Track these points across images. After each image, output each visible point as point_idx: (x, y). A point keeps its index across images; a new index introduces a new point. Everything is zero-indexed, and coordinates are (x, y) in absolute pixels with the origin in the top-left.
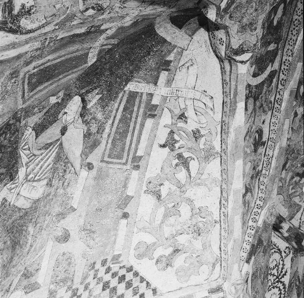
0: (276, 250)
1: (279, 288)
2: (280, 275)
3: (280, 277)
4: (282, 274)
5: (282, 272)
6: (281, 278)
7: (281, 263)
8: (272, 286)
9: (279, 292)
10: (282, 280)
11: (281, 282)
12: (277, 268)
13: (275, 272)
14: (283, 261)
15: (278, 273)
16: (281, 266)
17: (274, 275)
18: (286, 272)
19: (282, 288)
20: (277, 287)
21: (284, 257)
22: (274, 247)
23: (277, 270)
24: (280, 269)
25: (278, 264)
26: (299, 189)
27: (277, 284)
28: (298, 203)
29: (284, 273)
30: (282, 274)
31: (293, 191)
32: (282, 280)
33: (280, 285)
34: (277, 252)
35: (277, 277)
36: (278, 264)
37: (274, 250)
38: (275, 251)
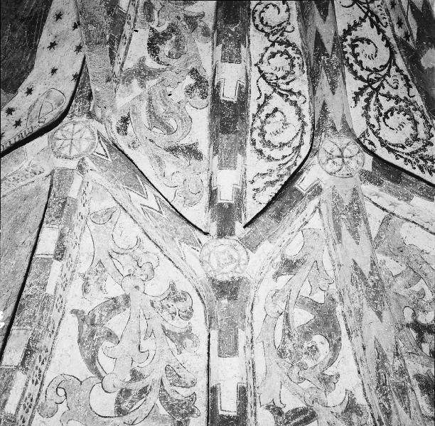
0: (400, 149)
1: (362, 69)
2: (371, 95)
3: (369, 90)
4: (365, 96)
5: (367, 100)
6: (366, 87)
7: (373, 121)
8: (383, 73)
9: (359, 59)
10: (361, 84)
11: (361, 78)
12: (383, 112)
13: (387, 105)
14: (368, 123)
15: (377, 100)
16: (373, 113)
17: (388, 96)
18: (356, 100)
19: (356, 67)
20: (368, 69)
21: (370, 131)
22: (409, 157)
23: (381, 106)
24: (372, 107)
25: (381, 118)
26: (402, 293)
27: (372, 77)
28: (388, 258)
29: (362, 99)
30: (365, 96)
31: (416, 288)
32: (361, 84)
33: (365, 74)
34: (393, 145)
35: (377, 90)
36: (381, 118)
37: (405, 151)
38: (403, 147)
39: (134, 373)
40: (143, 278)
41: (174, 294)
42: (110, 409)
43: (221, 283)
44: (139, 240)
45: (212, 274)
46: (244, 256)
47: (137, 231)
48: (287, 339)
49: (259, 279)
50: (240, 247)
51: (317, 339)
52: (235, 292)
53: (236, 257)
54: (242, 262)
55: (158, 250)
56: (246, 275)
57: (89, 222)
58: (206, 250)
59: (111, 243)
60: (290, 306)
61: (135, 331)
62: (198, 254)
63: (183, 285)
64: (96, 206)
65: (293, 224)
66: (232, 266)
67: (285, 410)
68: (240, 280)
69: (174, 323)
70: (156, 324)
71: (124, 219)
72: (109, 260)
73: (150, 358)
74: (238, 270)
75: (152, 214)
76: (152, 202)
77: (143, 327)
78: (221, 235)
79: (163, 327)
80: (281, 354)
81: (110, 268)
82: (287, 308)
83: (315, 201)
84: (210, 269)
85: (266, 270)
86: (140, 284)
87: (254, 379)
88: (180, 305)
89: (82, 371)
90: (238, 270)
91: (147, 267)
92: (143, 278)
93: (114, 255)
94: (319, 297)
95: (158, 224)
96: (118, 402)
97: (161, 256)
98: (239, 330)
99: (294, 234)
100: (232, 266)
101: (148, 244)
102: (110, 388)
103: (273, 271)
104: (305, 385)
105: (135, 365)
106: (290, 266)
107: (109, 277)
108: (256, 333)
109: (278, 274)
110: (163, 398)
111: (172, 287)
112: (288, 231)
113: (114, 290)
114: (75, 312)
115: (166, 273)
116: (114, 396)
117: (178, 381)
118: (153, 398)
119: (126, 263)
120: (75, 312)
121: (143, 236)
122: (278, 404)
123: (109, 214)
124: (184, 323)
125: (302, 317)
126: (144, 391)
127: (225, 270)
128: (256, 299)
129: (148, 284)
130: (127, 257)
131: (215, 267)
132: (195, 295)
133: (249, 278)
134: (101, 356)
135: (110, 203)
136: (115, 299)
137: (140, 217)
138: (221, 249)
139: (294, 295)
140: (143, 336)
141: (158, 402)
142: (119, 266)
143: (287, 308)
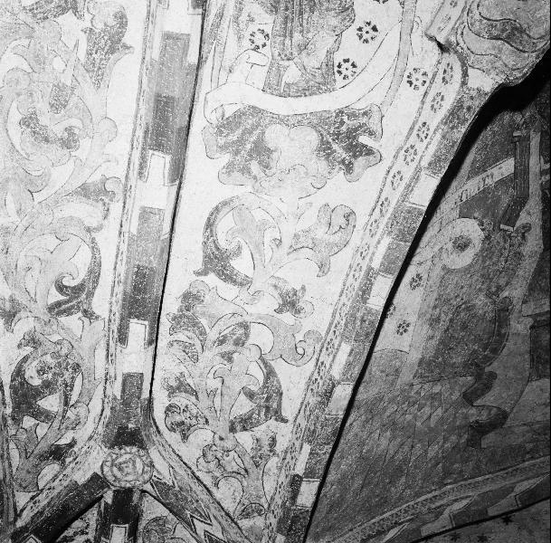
39: (230, 360)
40: (214, 448)
41: (184, 430)
42: (254, 329)
43: (134, 444)
44: (216, 485)
45: (142, 453)
46: (106, 469)
47: (218, 494)
48: (69, 381)
49: (92, 442)
50: (111, 479)
51: (36, 382)
52: (119, 435)
53: (115, 469)
54: (108, 464)
55: (198, 474)
56: (106, 450)
57: (266, 506)
58: (147, 477)
59: (245, 484)
60: (61, 414)
61: (226, 398)
62: (155, 473)
63: (173, 438)
64: (259, 522)
65: (48, 500)
66: (120, 460)
67: (80, 314)
68: (112, 447)
69: (185, 402)
70: (204, 402)
71: (229, 505)
72: (248, 467)
73: (213, 371)
74: (114, 456)
75: (201, 516)
76: (200, 527)
77: (217, 399)
78: (129, 491)
79: (197, 398)
80: (77, 367)
81: (247, 458)
82: (65, 411)
83: (20, 524)
84: (144, 458)
85: (83, 450)
86: (218, 442)
87: (108, 345)
88: (178, 418)
89: (281, 368)
90: (114, 456)
91: (210, 457)
92: (214, 448)
93: (243, 472)
94: (28, 422)
95: (195, 504)
96: (247, 335)
97: (194, 468)
98: (119, 398)
99: (47, 487)
100: (120, 460)
101: (208, 481)
102: (254, 348)
103: (76, 449)
104: (55, 338)
105: (228, 366)
106: (57, 454)
107: (249, 451)
108: (101, 388)
109: (71, 445)
110: (203, 333)
111: (185, 437)
112: (56, 492)
113: (245, 439)
114: (284, 421)
115: (190, 451)
116: (250, 341)
117: (186, 348)
118: (213, 335)
119: (232, 463)
120: (284, 421)
121: (214, 490)
122: (86, 321)
123: (246, 514)
124: (175, 401)
125: (51, 403)
126: (222, 342)
127: (128, 456)
128: (97, 421)
129: (209, 441)
130: (229, 470)
131: (138, 460)
132: (162, 427)
133: (103, 447)
134: (261, 378)
135: (245, 523)
136: (245, 429)
137: (213, 511)
138: (130, 478)
139: (56, 424)
140: (219, 391)
141: (208, 330)
142: (239, 461)
143: (65, 411)
